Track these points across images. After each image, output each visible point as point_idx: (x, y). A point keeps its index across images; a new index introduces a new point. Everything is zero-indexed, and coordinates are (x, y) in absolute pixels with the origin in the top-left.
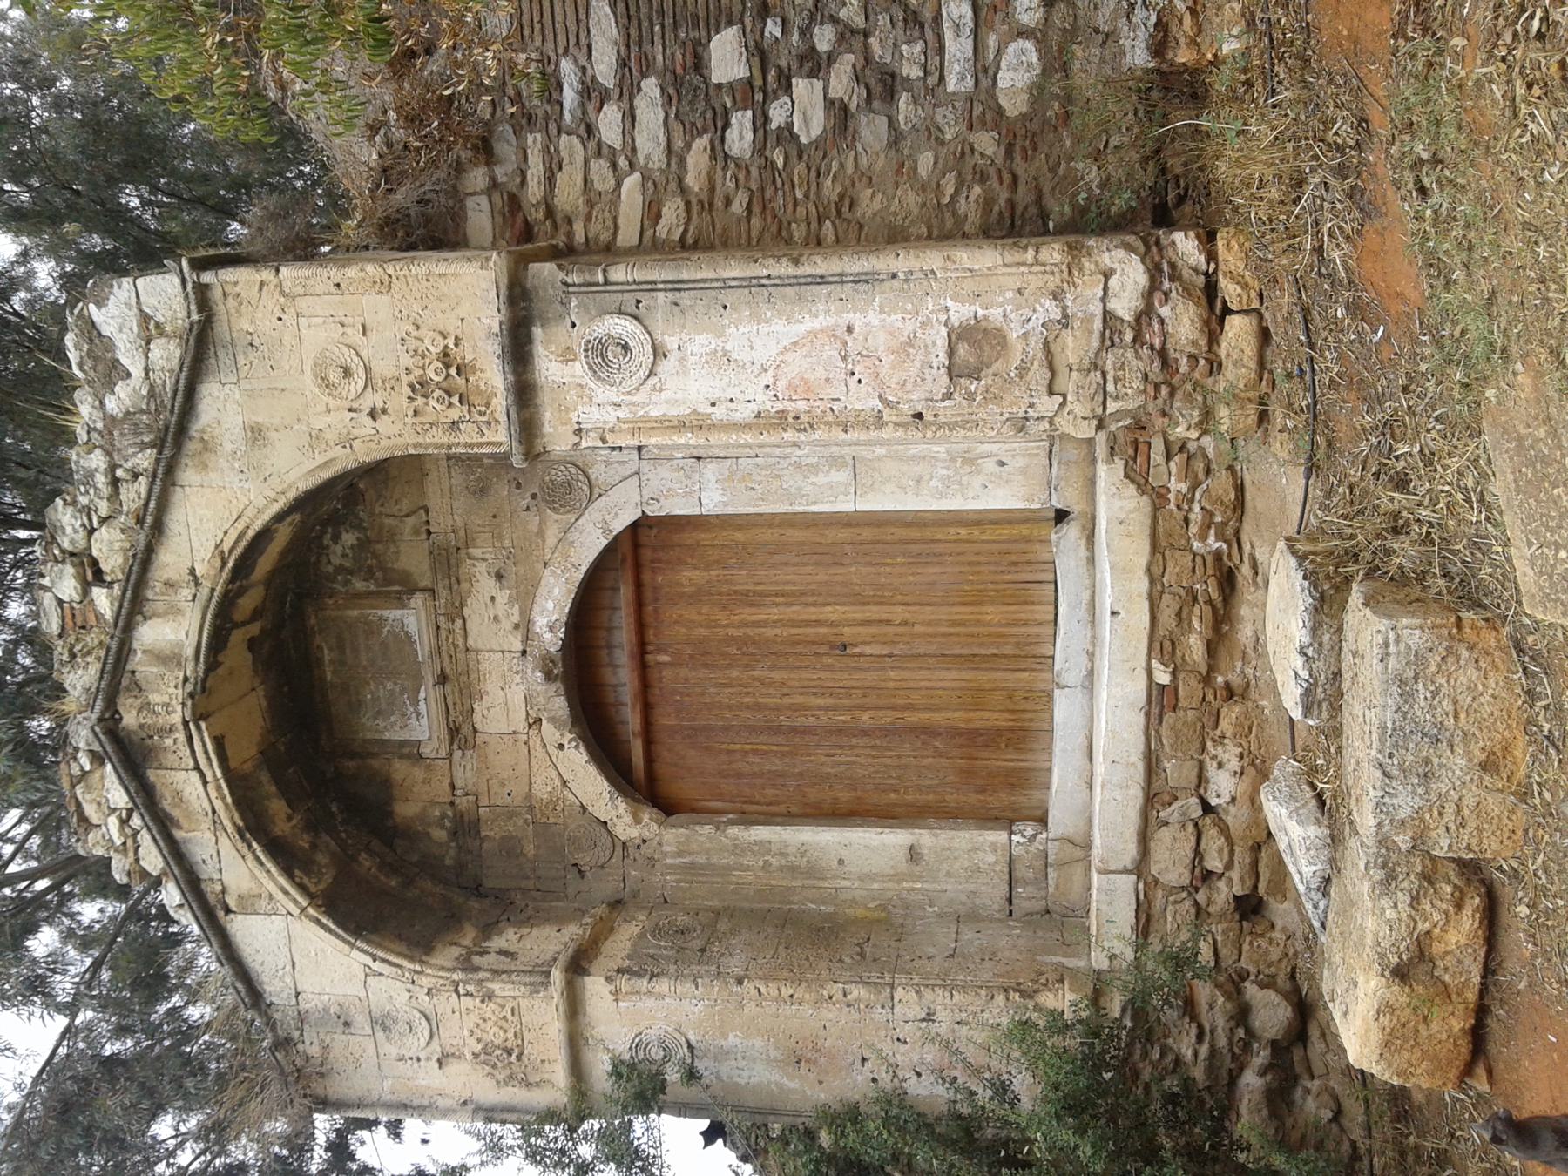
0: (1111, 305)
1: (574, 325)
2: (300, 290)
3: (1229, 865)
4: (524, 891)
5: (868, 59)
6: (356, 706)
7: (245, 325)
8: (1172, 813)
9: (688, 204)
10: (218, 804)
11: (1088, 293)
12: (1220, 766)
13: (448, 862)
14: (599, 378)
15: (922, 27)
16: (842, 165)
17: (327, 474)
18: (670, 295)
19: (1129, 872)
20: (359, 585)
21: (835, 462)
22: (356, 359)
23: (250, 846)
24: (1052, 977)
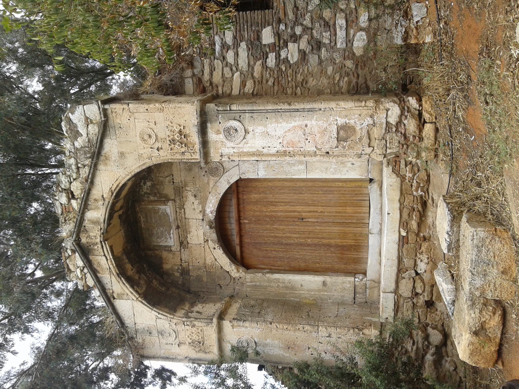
0: (388, 120)
1: (220, 123)
2: (135, 111)
3: (424, 291)
4: (203, 292)
5: (312, 37)
6: (151, 235)
7: (118, 121)
8: (406, 275)
9: (254, 82)
10: (111, 266)
11: (381, 116)
12: (421, 261)
13: (180, 283)
14: (228, 139)
15: (330, 27)
16: (303, 70)
17: (144, 167)
18: (250, 114)
19: (391, 292)
20: (152, 198)
21: (300, 162)
22: (153, 132)
23: (121, 279)
24: (368, 324)
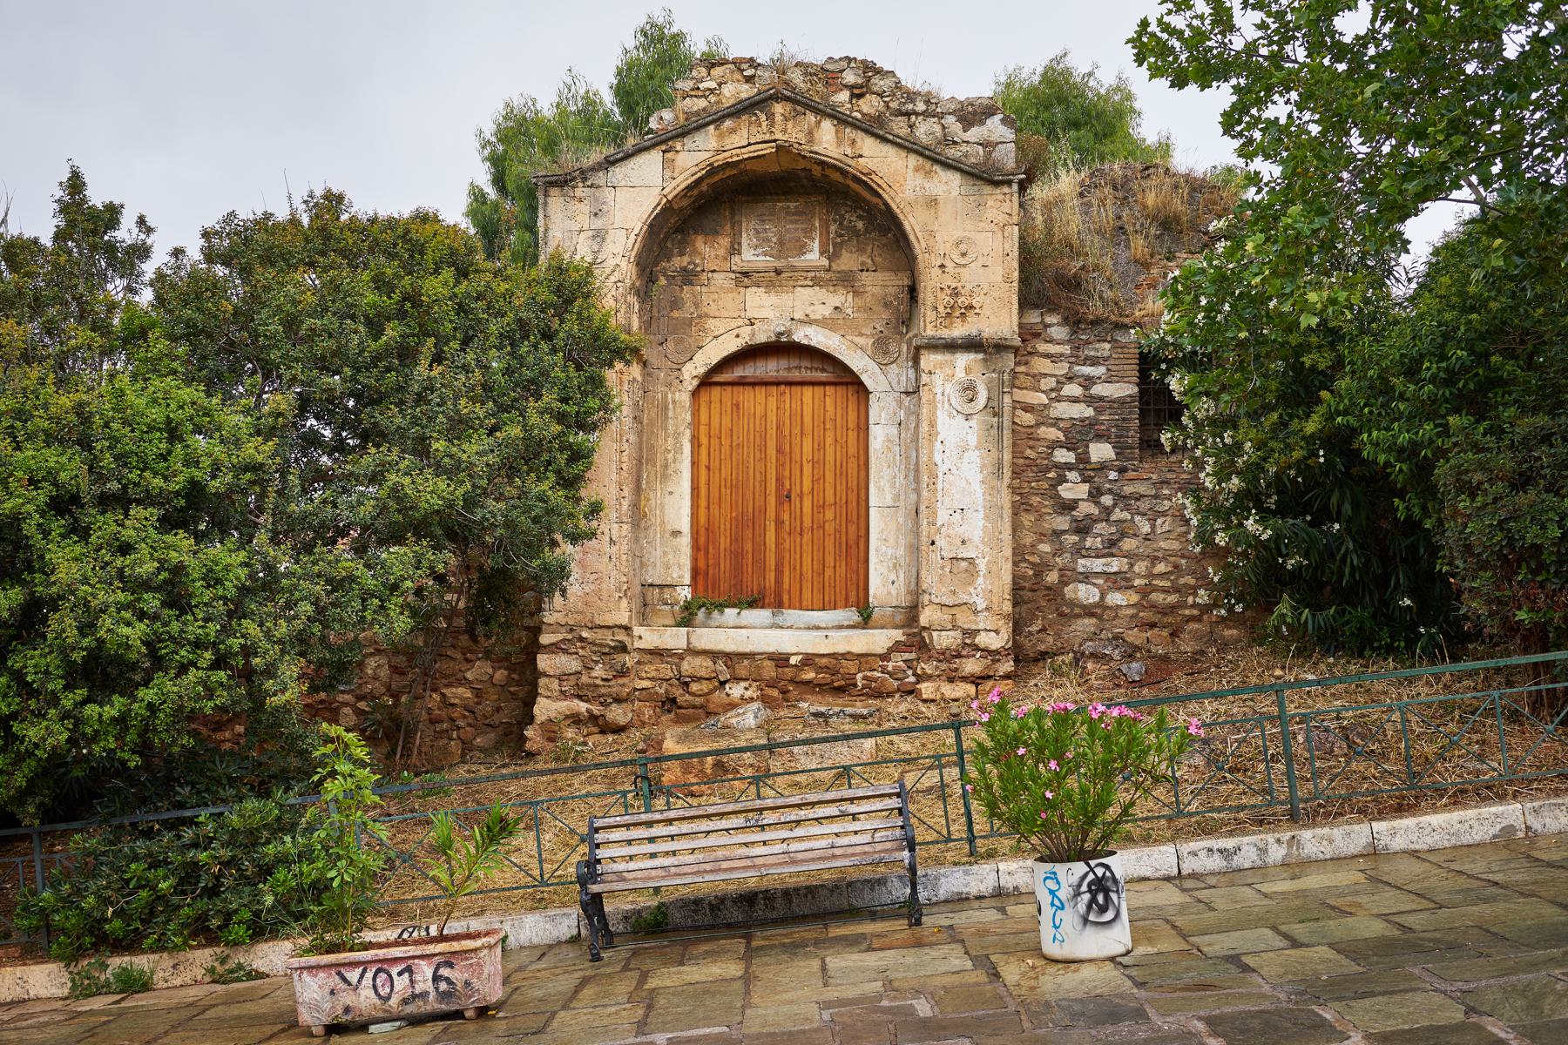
5: (1095, 521)
7: (990, 203)
8: (721, 666)
17: (912, 238)
20: (833, 228)
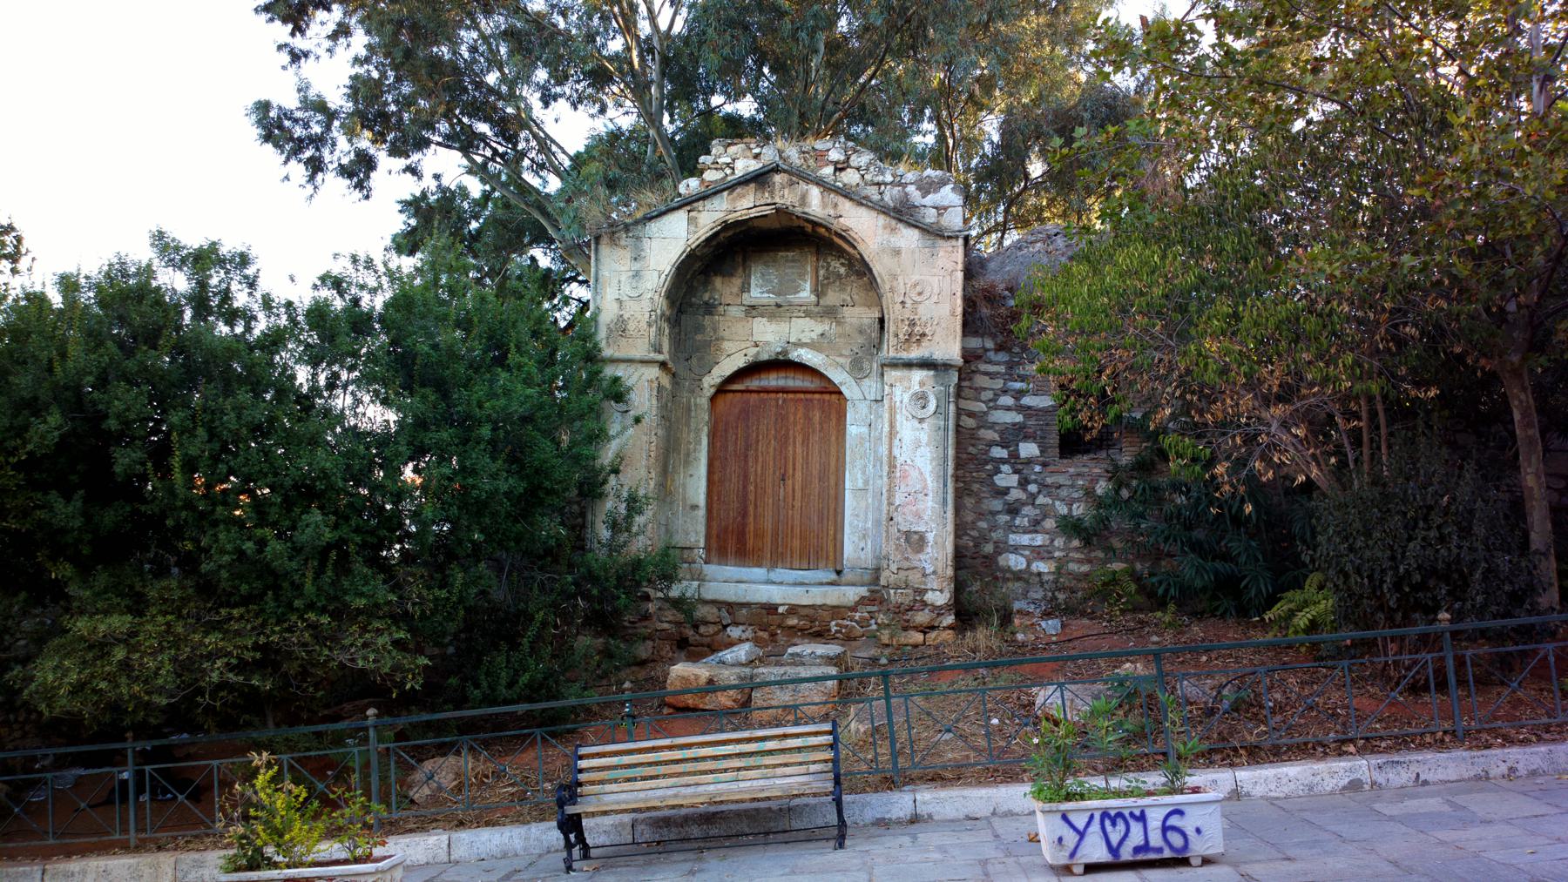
6: (766, 264)
8: (724, 613)
21: (866, 482)
